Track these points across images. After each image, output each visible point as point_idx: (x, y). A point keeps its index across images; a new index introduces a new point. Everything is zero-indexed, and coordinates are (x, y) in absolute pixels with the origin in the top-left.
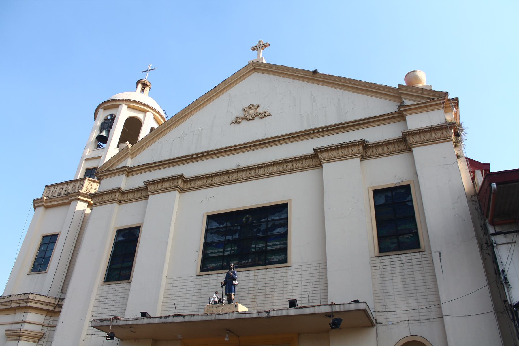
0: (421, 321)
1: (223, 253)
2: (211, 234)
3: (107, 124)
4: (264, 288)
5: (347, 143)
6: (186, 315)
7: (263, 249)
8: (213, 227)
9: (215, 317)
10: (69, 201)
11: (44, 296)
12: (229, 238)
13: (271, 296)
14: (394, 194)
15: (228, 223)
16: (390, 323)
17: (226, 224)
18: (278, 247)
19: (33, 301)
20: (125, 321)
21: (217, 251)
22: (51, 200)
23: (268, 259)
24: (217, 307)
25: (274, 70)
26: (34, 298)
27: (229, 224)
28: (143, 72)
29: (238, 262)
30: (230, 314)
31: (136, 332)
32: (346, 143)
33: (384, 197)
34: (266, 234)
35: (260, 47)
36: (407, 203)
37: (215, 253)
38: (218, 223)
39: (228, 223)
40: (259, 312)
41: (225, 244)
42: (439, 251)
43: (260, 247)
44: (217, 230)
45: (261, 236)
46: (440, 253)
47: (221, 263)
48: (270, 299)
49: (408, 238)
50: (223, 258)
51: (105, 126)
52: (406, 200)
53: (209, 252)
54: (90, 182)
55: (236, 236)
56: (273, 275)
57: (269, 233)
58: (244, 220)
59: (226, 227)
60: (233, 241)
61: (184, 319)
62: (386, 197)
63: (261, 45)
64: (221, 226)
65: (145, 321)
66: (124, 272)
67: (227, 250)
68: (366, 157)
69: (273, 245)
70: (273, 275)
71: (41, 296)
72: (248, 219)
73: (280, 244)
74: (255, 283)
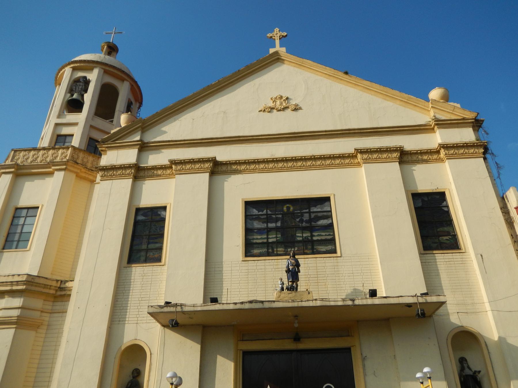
0: (468, 314)
2: (251, 220)
3: (81, 87)
4: (316, 276)
5: (388, 147)
6: (265, 301)
7: (308, 238)
8: (252, 214)
9: (298, 304)
11: (43, 278)
12: (271, 225)
13: (324, 284)
14: (429, 198)
15: (268, 211)
16: (441, 314)
17: (265, 211)
18: (323, 238)
19: (31, 283)
21: (259, 237)
23: (315, 249)
24: (289, 294)
25: (300, 64)
26: (33, 280)
27: (269, 212)
30: (313, 301)
32: (386, 147)
33: (421, 200)
34: (309, 224)
35: (277, 36)
36: (443, 208)
37: (257, 239)
38: (256, 210)
39: (268, 211)
40: (344, 300)
41: (268, 231)
42: (481, 253)
43: (305, 237)
44: (256, 216)
45: (305, 226)
46: (481, 256)
47: (266, 250)
48: (324, 286)
49: (447, 240)
50: (267, 244)
51: (77, 89)
52: (441, 206)
53: (250, 237)
54: (76, 151)
56: (324, 265)
57: (313, 223)
58: (285, 209)
59: (267, 214)
60: (276, 229)
61: (263, 305)
62: (423, 201)
63: (278, 34)
64: (260, 213)
66: (151, 254)
68: (401, 162)
69: (318, 235)
70: (324, 265)
71: (40, 278)
72: (288, 208)
73: (326, 235)
74: (307, 271)
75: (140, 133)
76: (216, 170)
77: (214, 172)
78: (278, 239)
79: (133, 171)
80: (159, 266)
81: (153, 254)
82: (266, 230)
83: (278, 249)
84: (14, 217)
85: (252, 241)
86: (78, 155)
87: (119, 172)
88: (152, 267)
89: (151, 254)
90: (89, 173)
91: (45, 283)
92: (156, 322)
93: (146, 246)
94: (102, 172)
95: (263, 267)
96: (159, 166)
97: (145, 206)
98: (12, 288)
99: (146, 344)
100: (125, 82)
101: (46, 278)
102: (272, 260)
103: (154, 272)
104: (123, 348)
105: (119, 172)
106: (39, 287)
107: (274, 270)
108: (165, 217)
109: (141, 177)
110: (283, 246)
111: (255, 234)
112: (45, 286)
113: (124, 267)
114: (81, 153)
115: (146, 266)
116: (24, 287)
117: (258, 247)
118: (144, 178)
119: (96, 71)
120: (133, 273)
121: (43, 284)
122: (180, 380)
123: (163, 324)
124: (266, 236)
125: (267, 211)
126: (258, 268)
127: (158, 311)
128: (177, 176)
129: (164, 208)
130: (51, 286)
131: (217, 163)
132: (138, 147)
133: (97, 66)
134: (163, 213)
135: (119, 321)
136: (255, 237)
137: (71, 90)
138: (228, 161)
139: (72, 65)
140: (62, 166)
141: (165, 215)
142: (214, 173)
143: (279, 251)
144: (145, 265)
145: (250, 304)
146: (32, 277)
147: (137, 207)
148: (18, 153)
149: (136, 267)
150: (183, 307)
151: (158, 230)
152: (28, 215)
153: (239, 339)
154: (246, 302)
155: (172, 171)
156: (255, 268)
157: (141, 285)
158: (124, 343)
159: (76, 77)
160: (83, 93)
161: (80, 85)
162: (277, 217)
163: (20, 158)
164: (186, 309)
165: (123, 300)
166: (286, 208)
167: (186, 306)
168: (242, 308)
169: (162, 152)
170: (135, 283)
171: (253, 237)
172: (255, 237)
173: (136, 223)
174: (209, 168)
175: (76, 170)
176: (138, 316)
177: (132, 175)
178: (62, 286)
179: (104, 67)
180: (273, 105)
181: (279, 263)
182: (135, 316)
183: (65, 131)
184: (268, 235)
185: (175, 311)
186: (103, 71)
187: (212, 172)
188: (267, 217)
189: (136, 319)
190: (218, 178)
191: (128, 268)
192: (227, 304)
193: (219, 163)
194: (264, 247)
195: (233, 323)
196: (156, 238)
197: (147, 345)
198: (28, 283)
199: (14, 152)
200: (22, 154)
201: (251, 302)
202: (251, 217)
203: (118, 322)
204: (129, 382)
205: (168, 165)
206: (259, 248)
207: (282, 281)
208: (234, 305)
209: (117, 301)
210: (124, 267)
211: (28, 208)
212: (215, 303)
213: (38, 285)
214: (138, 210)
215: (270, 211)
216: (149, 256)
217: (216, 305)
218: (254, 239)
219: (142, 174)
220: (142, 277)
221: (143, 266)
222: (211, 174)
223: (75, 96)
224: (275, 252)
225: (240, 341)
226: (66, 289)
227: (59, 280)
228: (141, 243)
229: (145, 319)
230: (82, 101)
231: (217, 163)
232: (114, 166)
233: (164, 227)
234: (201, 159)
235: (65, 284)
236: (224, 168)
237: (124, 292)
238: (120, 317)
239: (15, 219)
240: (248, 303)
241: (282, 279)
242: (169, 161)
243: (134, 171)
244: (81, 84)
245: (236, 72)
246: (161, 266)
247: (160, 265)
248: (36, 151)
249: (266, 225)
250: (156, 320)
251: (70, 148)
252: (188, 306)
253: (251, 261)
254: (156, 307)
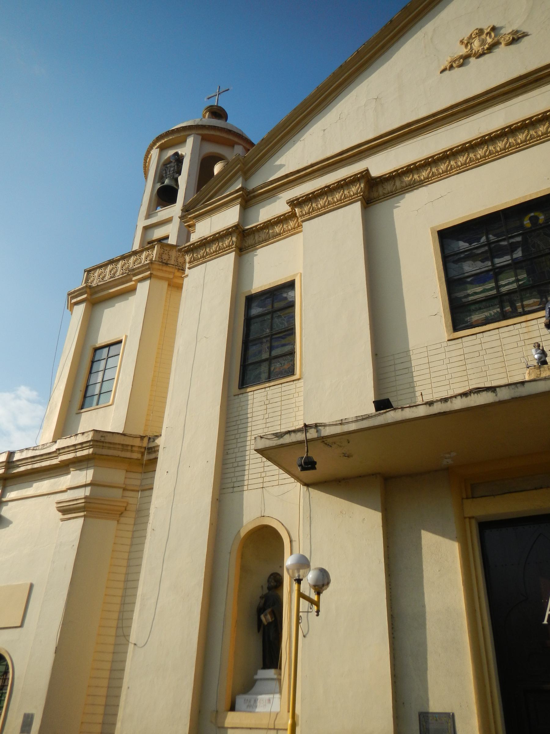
1: (495, 290)
2: (456, 262)
3: (172, 169)
10: (133, 283)
12: (502, 261)
15: (491, 236)
19: (101, 444)
20: (340, 427)
21: (479, 289)
22: (99, 288)
26: (102, 439)
27: (491, 237)
28: (209, 98)
29: (539, 300)
31: (352, 456)
38: (465, 242)
39: (491, 236)
47: (499, 310)
51: (168, 173)
54: (165, 248)
55: (518, 254)
58: (527, 222)
59: (489, 243)
60: (515, 265)
61: (496, 395)
64: (475, 244)
65: (391, 416)
66: (278, 365)
67: (504, 283)
71: (114, 434)
75: (240, 180)
76: (375, 195)
77: (372, 200)
78: (520, 283)
79: (234, 239)
80: (292, 383)
81: (280, 365)
82: (491, 273)
83: (525, 303)
84: (93, 362)
85: (464, 300)
86: (169, 255)
87: (214, 247)
88: (280, 386)
89: (277, 366)
91: (122, 443)
92: (296, 481)
93: (268, 353)
94: (190, 256)
95: (498, 343)
96: (275, 218)
97: (260, 290)
98: (76, 455)
99: (280, 522)
100: (236, 147)
102: (515, 324)
103: (283, 394)
104: (243, 533)
105: (213, 248)
106: (114, 449)
107: (522, 343)
108: (294, 300)
109: (249, 247)
110: (535, 293)
111: (468, 286)
112: (124, 447)
113: (234, 396)
114: (173, 250)
115: (270, 387)
116: (91, 451)
117: (480, 309)
118: (254, 247)
119: (190, 141)
120: (250, 402)
121: (119, 444)
122: (323, 575)
123: (306, 481)
124: (493, 285)
125: (487, 238)
126: (485, 346)
127: (274, 445)
128: (304, 224)
129: (291, 285)
130: (132, 446)
131: (374, 181)
132: (239, 200)
133: (191, 133)
134: (290, 294)
135: (233, 487)
136: (469, 292)
137: (160, 177)
138: (395, 171)
139: (158, 144)
140: (145, 272)
141: (294, 296)
142: (372, 201)
143: (529, 305)
144: (267, 385)
145: (464, 399)
146: (101, 434)
147: (247, 295)
148: (92, 273)
149: (254, 391)
150: (320, 429)
151: (286, 323)
152: (110, 355)
153: (464, 496)
154: (455, 397)
155: (297, 221)
156: (478, 348)
157: (264, 421)
158: (244, 525)
159: (166, 158)
160: (176, 175)
161: (170, 167)
162: (512, 243)
163: (95, 281)
164: (326, 432)
165: (236, 450)
166: (529, 221)
167: (325, 425)
168: (448, 410)
169: (280, 198)
170: (254, 419)
171: (465, 292)
172: (469, 292)
173: (248, 321)
174: (360, 193)
175: (166, 275)
176: (263, 475)
177: (234, 246)
178: (152, 445)
179: (200, 132)
180: (468, 50)
181: (531, 329)
182: (259, 475)
183: (158, 233)
184: (497, 282)
185: (305, 439)
186: (200, 137)
187: (368, 201)
188: (490, 250)
189: (261, 480)
190: (381, 208)
191: (240, 396)
192: (411, 408)
193: (378, 180)
194: (492, 306)
195: (447, 462)
196: (283, 338)
197: (282, 524)
198: (96, 443)
199: (88, 274)
200: (98, 272)
201: (465, 394)
202: (456, 258)
203: (231, 490)
204: (261, 598)
205: (289, 213)
206: (483, 309)
207: (541, 348)
208: (428, 406)
209: (227, 454)
210: (234, 396)
211: (109, 346)
212: (385, 411)
213: (112, 446)
214: (250, 299)
215: (494, 235)
216: (274, 369)
217: (388, 414)
218: (469, 295)
219: (250, 241)
220: (265, 407)
221: (265, 388)
222: (365, 204)
223: (167, 182)
224: (520, 310)
225: (467, 498)
227: (144, 437)
228: (260, 352)
229: (276, 478)
230: (175, 187)
231: (374, 181)
232: (205, 239)
233: (293, 317)
234: (342, 180)
235: (154, 441)
236: (389, 187)
237: (238, 436)
238: (234, 480)
239: (95, 364)
240: (459, 397)
241: (539, 346)
242: (287, 203)
243: (237, 238)
244: (172, 164)
245: (386, 26)
246: (295, 382)
247: (293, 381)
248: (113, 264)
249: (489, 263)
250: (295, 479)
251: (156, 246)
252: (330, 425)
253: (468, 336)
254: (269, 437)
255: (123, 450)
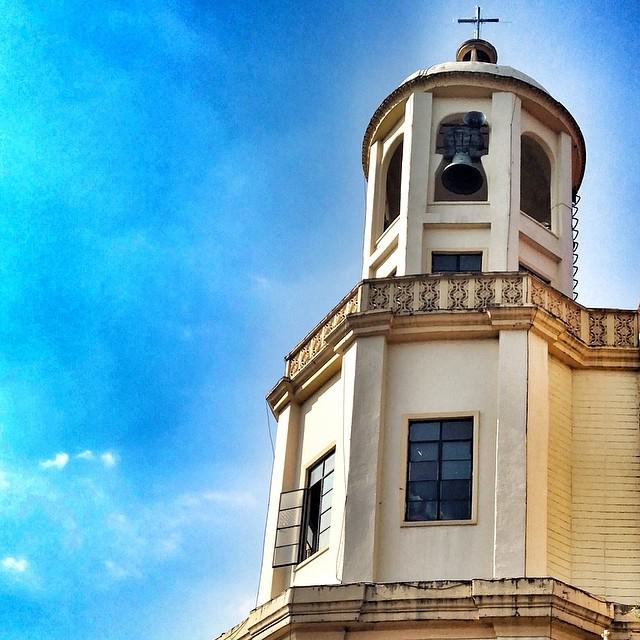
51: (459, 143)
90: (573, 344)
101: (588, 594)
133: (499, 88)
178: (620, 618)
226: (629, 626)
251: (524, 279)
255: (587, 619)
